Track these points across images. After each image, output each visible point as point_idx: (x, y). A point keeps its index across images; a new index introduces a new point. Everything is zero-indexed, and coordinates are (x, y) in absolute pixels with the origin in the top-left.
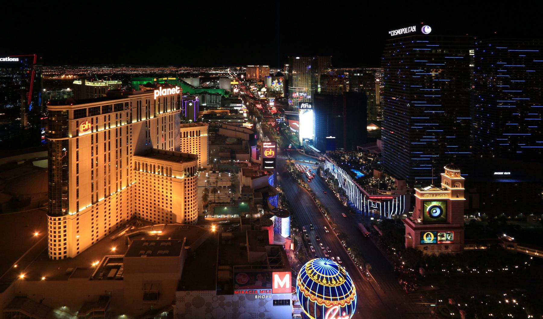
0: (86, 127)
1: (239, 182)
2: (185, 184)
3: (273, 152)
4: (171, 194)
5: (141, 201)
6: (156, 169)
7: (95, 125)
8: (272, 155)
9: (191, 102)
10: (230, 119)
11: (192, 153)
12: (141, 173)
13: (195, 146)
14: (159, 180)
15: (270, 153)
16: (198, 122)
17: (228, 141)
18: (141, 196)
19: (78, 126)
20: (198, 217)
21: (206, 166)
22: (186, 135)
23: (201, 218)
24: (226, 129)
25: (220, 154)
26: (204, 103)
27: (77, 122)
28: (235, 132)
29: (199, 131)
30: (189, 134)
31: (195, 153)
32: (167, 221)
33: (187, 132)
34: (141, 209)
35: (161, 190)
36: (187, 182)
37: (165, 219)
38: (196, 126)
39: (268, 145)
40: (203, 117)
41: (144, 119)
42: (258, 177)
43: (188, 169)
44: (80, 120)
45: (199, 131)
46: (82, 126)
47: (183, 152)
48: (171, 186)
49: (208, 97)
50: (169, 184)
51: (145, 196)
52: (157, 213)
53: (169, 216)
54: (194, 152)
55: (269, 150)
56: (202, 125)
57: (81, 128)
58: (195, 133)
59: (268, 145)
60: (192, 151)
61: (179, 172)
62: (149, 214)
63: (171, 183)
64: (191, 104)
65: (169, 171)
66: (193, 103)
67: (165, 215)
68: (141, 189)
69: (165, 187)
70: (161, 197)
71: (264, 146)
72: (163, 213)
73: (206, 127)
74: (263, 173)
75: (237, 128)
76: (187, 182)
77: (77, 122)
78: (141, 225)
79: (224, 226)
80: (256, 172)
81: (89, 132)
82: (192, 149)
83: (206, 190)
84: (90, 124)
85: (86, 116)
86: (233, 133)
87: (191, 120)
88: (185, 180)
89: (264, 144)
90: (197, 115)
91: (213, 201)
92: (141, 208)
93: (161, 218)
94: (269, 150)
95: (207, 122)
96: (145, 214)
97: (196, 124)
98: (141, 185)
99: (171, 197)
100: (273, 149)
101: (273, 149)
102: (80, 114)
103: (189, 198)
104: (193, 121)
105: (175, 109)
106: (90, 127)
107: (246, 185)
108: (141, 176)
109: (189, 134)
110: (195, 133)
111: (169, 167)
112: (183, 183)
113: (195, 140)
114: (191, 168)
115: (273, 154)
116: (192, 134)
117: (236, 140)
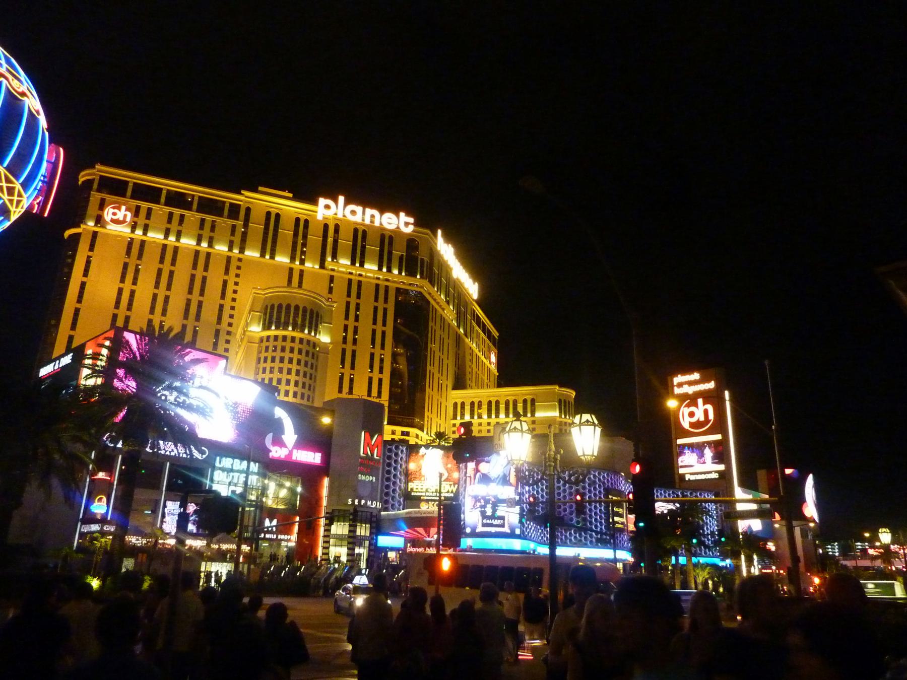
0: (120, 215)
3: (710, 408)
7: (142, 220)
8: (707, 420)
15: (699, 416)
19: (102, 205)
39: (691, 383)
41: (282, 259)
44: (109, 198)
46: (112, 211)
57: (108, 214)
59: (691, 383)
81: (125, 230)
84: (129, 215)
85: (124, 196)
89: (677, 380)
101: (707, 397)
102: (117, 188)
105: (395, 272)
106: (128, 219)
115: (711, 416)
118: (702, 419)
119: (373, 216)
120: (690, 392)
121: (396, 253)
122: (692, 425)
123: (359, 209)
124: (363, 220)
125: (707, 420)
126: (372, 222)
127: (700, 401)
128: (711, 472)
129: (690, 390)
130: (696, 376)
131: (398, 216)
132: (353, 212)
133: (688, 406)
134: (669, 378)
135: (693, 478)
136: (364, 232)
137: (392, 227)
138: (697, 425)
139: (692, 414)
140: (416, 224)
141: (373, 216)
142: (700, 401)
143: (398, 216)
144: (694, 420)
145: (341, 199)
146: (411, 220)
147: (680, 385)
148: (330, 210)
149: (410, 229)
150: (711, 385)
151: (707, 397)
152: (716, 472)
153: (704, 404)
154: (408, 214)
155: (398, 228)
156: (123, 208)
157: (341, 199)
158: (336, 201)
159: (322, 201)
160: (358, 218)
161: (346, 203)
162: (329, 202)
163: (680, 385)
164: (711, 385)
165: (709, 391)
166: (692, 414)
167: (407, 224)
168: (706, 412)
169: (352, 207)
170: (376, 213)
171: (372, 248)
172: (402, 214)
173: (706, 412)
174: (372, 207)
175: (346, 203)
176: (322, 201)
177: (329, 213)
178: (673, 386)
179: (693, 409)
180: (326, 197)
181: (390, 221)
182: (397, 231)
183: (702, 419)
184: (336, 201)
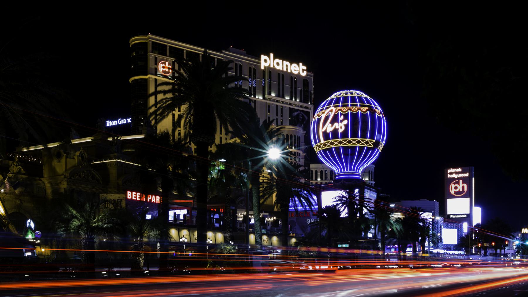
3: (465, 185)
15: (460, 188)
27: (156, 58)
39: (457, 173)
44: (159, 57)
59: (457, 173)
77: (156, 58)
89: (450, 171)
101: (464, 180)
115: (466, 189)
118: (461, 190)
119: (287, 66)
120: (456, 177)
121: (299, 89)
122: (455, 193)
123: (280, 61)
124: (283, 68)
126: (287, 69)
127: (461, 181)
128: (463, 215)
129: (456, 176)
130: (460, 170)
131: (299, 65)
132: (278, 64)
133: (454, 184)
134: (445, 169)
135: (454, 217)
136: (283, 75)
137: (296, 73)
140: (307, 70)
141: (287, 66)
142: (461, 181)
143: (299, 65)
145: (272, 55)
146: (305, 68)
147: (451, 173)
148: (267, 62)
149: (304, 74)
150: (467, 175)
151: (464, 180)
152: (465, 214)
153: (463, 183)
154: (303, 65)
155: (299, 73)
156: (167, 63)
157: (272, 55)
159: (263, 57)
160: (279, 68)
161: (275, 58)
162: (266, 57)
163: (451, 173)
164: (467, 175)
165: (466, 177)
166: (456, 188)
167: (303, 70)
168: (463, 187)
169: (277, 60)
170: (288, 63)
171: (287, 86)
172: (301, 64)
173: (463, 187)
174: (286, 61)
175: (275, 58)
176: (263, 57)
177: (267, 65)
178: (447, 174)
179: (456, 185)
180: (265, 55)
181: (295, 69)
182: (299, 75)
183: (461, 190)
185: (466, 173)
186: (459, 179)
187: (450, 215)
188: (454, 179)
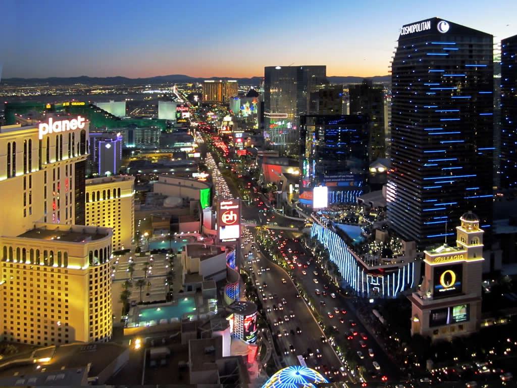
1: (182, 267)
2: (91, 277)
3: (235, 216)
4: (67, 295)
5: (15, 312)
6: (42, 256)
8: (233, 220)
9: (109, 142)
10: (172, 168)
11: (107, 226)
12: (15, 266)
13: (112, 215)
14: (45, 275)
15: (231, 218)
16: (119, 174)
17: (168, 203)
18: (15, 303)
20: (113, 328)
21: (129, 246)
22: (96, 196)
23: (118, 329)
24: (165, 183)
25: (153, 224)
26: (130, 142)
28: (179, 187)
29: (119, 190)
30: (101, 195)
31: (112, 226)
32: (60, 341)
33: (98, 193)
34: (15, 326)
35: (49, 290)
36: (94, 274)
37: (56, 337)
38: (114, 181)
39: (228, 205)
40: (129, 166)
42: (211, 256)
43: (96, 252)
45: (119, 190)
47: (91, 225)
48: (66, 283)
49: (137, 132)
50: (63, 280)
51: (22, 304)
52: (42, 330)
53: (63, 333)
54: (108, 223)
55: (229, 213)
56: (124, 180)
58: (112, 193)
59: (228, 205)
60: (106, 223)
61: (80, 258)
62: (29, 333)
63: (66, 277)
64: (108, 146)
65: (64, 258)
66: (112, 145)
67: (56, 332)
68: (15, 292)
69: (56, 285)
70: (49, 302)
71: (222, 208)
72: (53, 328)
73: (132, 182)
74: (219, 249)
75: (182, 182)
76: (94, 274)
78: (15, 352)
79: (154, 337)
80: (208, 248)
82: (106, 219)
83: (128, 284)
86: (177, 189)
87: (108, 173)
88: (91, 271)
89: (222, 204)
90: (119, 163)
91: (138, 301)
92: (15, 323)
93: (49, 336)
94: (229, 213)
95: (135, 174)
96: (22, 332)
97: (114, 179)
98: (15, 286)
99: (67, 301)
100: (234, 211)
101: (234, 211)
103: (96, 299)
104: (112, 174)
107: (192, 271)
108: (15, 270)
109: (101, 195)
110: (112, 193)
111: (63, 252)
112: (87, 277)
113: (112, 204)
114: (101, 250)
115: (235, 219)
116: (107, 194)
117: (180, 201)
122: (227, 221)
125: (233, 220)
127: (232, 212)
129: (228, 208)
132: (57, 127)
133: (226, 214)
135: (225, 241)
138: (230, 221)
139: (227, 217)
141: (66, 124)
142: (232, 212)
143: (77, 119)
144: (228, 219)
145: (51, 120)
147: (223, 206)
150: (237, 207)
157: (51, 120)
158: (48, 123)
161: (54, 121)
162: (45, 125)
163: (223, 206)
165: (235, 209)
166: (227, 217)
168: (234, 217)
170: (67, 122)
172: (79, 117)
173: (234, 217)
175: (54, 121)
176: (41, 126)
178: (220, 206)
179: (228, 215)
184: (48, 123)
185: (236, 205)
186: (230, 210)
187: (222, 240)
188: (226, 210)
